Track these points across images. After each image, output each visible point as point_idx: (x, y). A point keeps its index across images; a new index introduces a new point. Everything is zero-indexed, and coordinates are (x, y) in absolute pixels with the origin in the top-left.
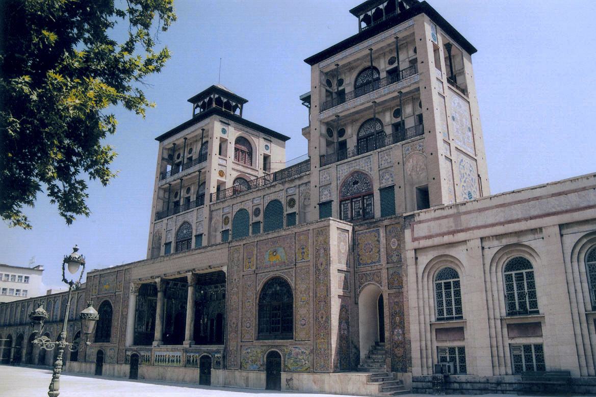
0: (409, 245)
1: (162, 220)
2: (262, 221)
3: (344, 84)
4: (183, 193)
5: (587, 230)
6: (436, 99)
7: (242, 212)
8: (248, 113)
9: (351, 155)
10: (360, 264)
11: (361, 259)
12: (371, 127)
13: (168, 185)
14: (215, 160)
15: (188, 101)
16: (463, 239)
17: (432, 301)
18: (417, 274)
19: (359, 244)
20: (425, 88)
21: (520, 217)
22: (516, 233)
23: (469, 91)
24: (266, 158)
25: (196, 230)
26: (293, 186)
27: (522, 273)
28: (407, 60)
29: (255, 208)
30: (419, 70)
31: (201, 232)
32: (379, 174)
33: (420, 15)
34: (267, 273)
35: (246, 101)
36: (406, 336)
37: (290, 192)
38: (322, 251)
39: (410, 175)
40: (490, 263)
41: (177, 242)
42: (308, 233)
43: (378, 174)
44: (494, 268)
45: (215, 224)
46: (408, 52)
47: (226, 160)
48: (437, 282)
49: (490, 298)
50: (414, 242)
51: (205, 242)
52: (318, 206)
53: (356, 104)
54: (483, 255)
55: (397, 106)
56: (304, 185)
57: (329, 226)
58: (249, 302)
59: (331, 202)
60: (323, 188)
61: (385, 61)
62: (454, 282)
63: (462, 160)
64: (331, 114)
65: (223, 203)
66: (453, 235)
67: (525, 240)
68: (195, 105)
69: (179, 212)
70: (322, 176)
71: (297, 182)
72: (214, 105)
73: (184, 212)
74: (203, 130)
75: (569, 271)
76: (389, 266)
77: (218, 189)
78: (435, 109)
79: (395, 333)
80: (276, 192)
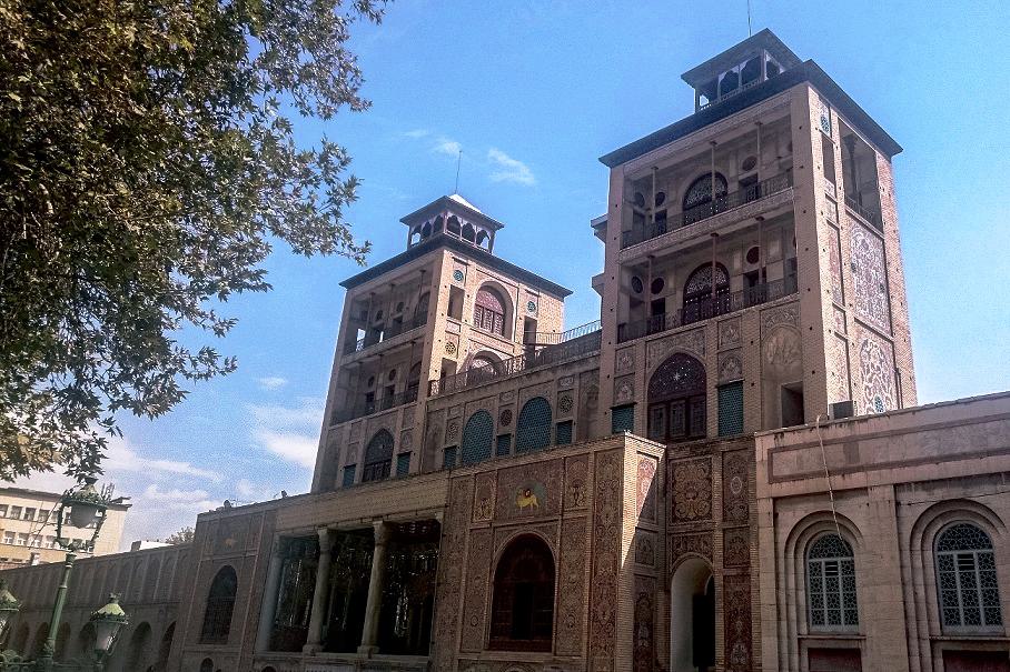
0: (764, 490)
2: (513, 433)
3: (665, 202)
4: (381, 380)
6: (822, 230)
10: (675, 519)
14: (441, 323)
15: (401, 221)
17: (802, 594)
18: (776, 543)
21: (967, 449)
22: (959, 478)
27: (971, 556)
28: (776, 162)
29: (503, 409)
36: (755, 658)
37: (566, 385)
38: (609, 491)
41: (366, 466)
44: (918, 543)
48: (814, 560)
49: (911, 599)
51: (414, 465)
56: (590, 374)
57: (622, 448)
59: (632, 405)
61: (737, 164)
62: (843, 563)
63: (866, 342)
67: (978, 494)
71: (577, 369)
72: (445, 232)
77: (443, 374)
78: (820, 251)
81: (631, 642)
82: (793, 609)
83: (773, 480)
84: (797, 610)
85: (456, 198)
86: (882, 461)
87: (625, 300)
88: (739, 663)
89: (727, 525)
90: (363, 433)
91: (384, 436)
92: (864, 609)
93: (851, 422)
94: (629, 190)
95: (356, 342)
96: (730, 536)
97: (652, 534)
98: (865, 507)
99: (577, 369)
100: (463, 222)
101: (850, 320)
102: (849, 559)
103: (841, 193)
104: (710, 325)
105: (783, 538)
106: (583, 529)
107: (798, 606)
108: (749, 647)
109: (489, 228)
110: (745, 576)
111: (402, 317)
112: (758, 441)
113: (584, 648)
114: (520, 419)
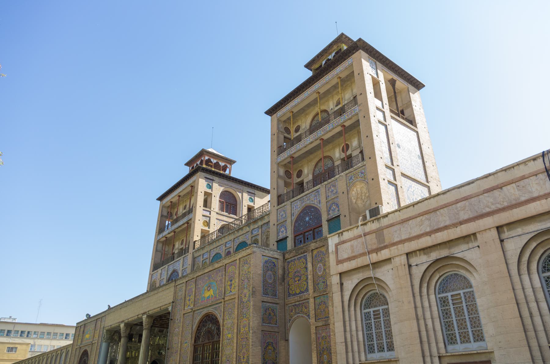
0: (334, 269)
1: (157, 270)
5: (536, 229)
8: (235, 172)
10: (290, 295)
11: (291, 289)
13: (164, 239)
14: (200, 211)
15: (185, 165)
16: (388, 257)
17: (360, 333)
18: (343, 302)
20: (364, 117)
21: (448, 223)
23: (417, 122)
24: (250, 209)
27: (460, 294)
29: (227, 251)
32: (327, 206)
34: (202, 310)
35: (234, 162)
37: (255, 233)
38: (246, 280)
39: (355, 203)
40: (419, 283)
43: (326, 205)
44: (425, 290)
47: (210, 212)
50: (338, 265)
52: (276, 243)
53: (306, 143)
54: (410, 274)
56: (266, 225)
58: (186, 343)
59: (286, 238)
60: (280, 225)
64: (286, 156)
65: (203, 250)
66: (377, 253)
68: (191, 168)
70: (280, 214)
71: (260, 223)
74: (192, 186)
75: (518, 286)
80: (243, 234)
82: (355, 344)
83: (339, 262)
84: (358, 345)
85: (210, 150)
86: (398, 240)
87: (281, 183)
91: (175, 271)
92: (397, 340)
93: (378, 219)
94: (281, 125)
96: (318, 301)
97: (274, 305)
98: (391, 271)
100: (214, 161)
101: (398, 174)
102: (386, 307)
103: (387, 108)
104: (321, 187)
105: (346, 298)
107: (358, 342)
109: (228, 163)
110: (327, 325)
112: (330, 240)
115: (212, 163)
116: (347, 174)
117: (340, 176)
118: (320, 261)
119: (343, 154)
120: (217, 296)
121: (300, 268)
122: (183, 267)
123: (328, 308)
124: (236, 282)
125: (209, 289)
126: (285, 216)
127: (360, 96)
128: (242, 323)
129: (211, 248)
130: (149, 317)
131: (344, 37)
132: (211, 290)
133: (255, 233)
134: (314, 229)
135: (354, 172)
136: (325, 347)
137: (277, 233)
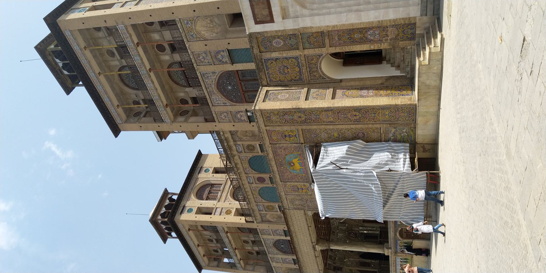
1: (273, 267)
2: (269, 175)
3: (137, 100)
4: (249, 248)
7: (262, 193)
8: (176, 188)
9: (202, 92)
10: (300, 79)
11: (295, 77)
12: (177, 74)
13: (241, 261)
14: (214, 218)
19: (280, 80)
20: (130, 18)
24: (217, 171)
25: (280, 235)
26: (235, 147)
28: (107, 38)
29: (257, 182)
30: (113, 25)
31: (282, 231)
33: (59, 24)
35: (166, 190)
37: (241, 149)
38: (286, 117)
41: (293, 254)
42: (269, 131)
45: (274, 218)
46: (100, 38)
53: (153, 89)
55: (153, 48)
56: (234, 136)
57: (261, 111)
68: (169, 237)
69: (265, 251)
70: (224, 120)
71: (232, 143)
73: (265, 247)
74: (189, 230)
76: (301, 47)
77: (242, 215)
79: (372, 38)
81: (370, 99)
87: (193, 119)
88: (379, 34)
89: (301, 47)
90: (276, 256)
95: (229, 263)
99: (232, 143)
104: (200, 70)
106: (309, 130)
108: (370, 29)
109: (167, 196)
111: (215, 239)
113: (376, 126)
114: (260, 172)
115: (165, 213)
116: (187, 40)
117: (189, 48)
118: (270, 43)
119: (166, 51)
120: (300, 153)
121: (276, 67)
122: (271, 235)
123: (313, 33)
124: (286, 128)
125: (292, 164)
126: (227, 113)
127: (107, 22)
128: (324, 120)
129: (254, 202)
130: (318, 242)
131: (38, 47)
132: (294, 161)
133: (241, 149)
134: (240, 80)
135: (186, 32)
136: (348, 37)
137: (242, 122)
